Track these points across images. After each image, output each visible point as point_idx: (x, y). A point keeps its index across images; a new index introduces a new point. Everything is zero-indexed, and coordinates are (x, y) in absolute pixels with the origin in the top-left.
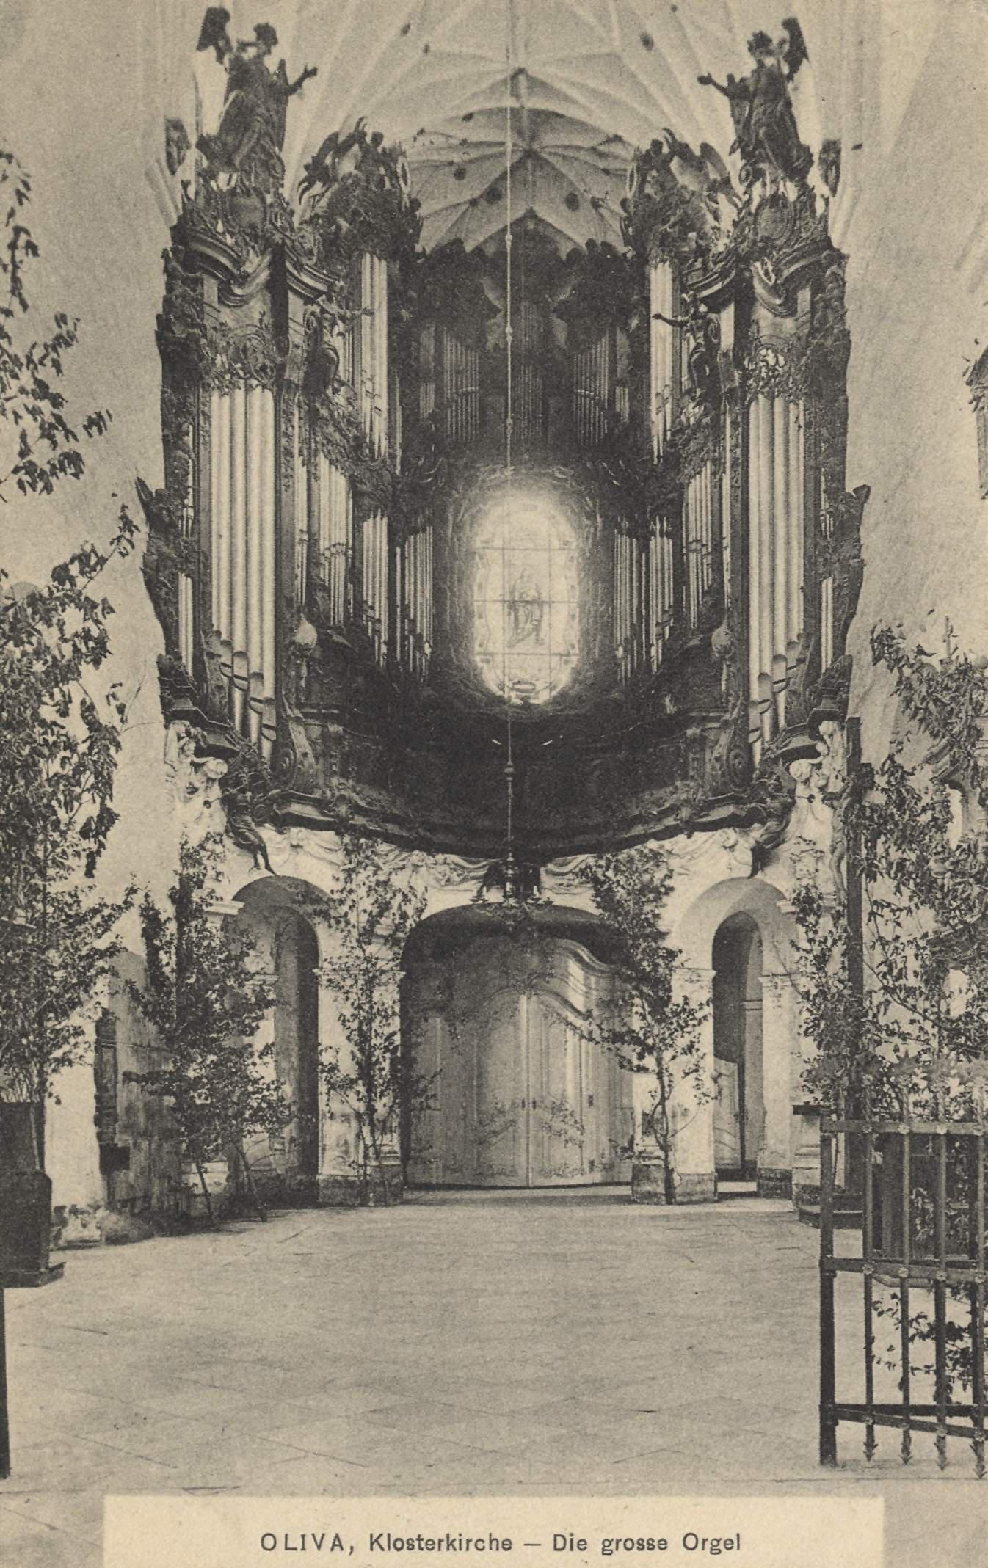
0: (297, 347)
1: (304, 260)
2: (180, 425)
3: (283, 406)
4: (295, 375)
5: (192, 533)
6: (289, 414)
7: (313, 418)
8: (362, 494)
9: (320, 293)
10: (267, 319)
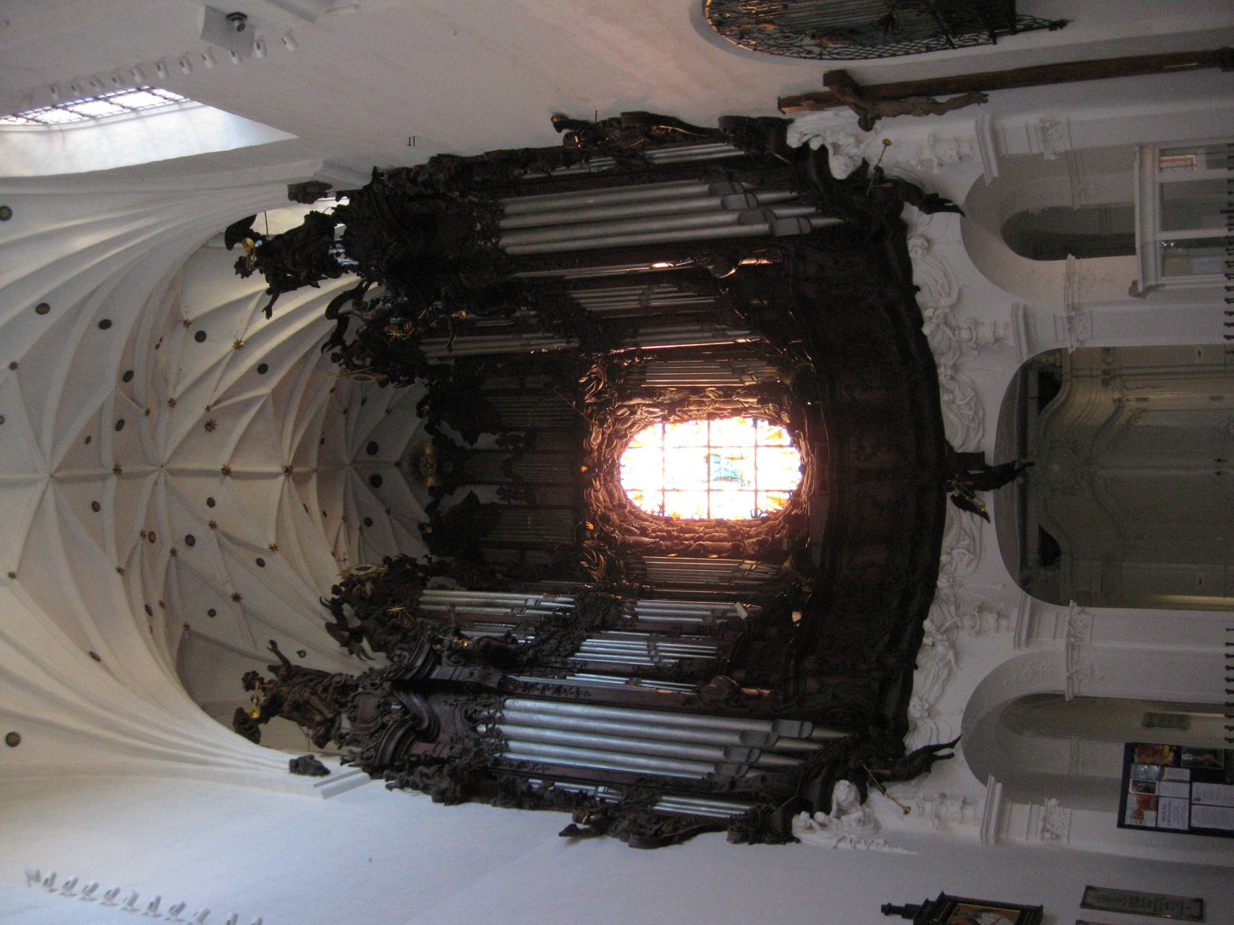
0: (472, 674)
1: (406, 661)
3: (520, 691)
7: (535, 664)
10: (451, 699)
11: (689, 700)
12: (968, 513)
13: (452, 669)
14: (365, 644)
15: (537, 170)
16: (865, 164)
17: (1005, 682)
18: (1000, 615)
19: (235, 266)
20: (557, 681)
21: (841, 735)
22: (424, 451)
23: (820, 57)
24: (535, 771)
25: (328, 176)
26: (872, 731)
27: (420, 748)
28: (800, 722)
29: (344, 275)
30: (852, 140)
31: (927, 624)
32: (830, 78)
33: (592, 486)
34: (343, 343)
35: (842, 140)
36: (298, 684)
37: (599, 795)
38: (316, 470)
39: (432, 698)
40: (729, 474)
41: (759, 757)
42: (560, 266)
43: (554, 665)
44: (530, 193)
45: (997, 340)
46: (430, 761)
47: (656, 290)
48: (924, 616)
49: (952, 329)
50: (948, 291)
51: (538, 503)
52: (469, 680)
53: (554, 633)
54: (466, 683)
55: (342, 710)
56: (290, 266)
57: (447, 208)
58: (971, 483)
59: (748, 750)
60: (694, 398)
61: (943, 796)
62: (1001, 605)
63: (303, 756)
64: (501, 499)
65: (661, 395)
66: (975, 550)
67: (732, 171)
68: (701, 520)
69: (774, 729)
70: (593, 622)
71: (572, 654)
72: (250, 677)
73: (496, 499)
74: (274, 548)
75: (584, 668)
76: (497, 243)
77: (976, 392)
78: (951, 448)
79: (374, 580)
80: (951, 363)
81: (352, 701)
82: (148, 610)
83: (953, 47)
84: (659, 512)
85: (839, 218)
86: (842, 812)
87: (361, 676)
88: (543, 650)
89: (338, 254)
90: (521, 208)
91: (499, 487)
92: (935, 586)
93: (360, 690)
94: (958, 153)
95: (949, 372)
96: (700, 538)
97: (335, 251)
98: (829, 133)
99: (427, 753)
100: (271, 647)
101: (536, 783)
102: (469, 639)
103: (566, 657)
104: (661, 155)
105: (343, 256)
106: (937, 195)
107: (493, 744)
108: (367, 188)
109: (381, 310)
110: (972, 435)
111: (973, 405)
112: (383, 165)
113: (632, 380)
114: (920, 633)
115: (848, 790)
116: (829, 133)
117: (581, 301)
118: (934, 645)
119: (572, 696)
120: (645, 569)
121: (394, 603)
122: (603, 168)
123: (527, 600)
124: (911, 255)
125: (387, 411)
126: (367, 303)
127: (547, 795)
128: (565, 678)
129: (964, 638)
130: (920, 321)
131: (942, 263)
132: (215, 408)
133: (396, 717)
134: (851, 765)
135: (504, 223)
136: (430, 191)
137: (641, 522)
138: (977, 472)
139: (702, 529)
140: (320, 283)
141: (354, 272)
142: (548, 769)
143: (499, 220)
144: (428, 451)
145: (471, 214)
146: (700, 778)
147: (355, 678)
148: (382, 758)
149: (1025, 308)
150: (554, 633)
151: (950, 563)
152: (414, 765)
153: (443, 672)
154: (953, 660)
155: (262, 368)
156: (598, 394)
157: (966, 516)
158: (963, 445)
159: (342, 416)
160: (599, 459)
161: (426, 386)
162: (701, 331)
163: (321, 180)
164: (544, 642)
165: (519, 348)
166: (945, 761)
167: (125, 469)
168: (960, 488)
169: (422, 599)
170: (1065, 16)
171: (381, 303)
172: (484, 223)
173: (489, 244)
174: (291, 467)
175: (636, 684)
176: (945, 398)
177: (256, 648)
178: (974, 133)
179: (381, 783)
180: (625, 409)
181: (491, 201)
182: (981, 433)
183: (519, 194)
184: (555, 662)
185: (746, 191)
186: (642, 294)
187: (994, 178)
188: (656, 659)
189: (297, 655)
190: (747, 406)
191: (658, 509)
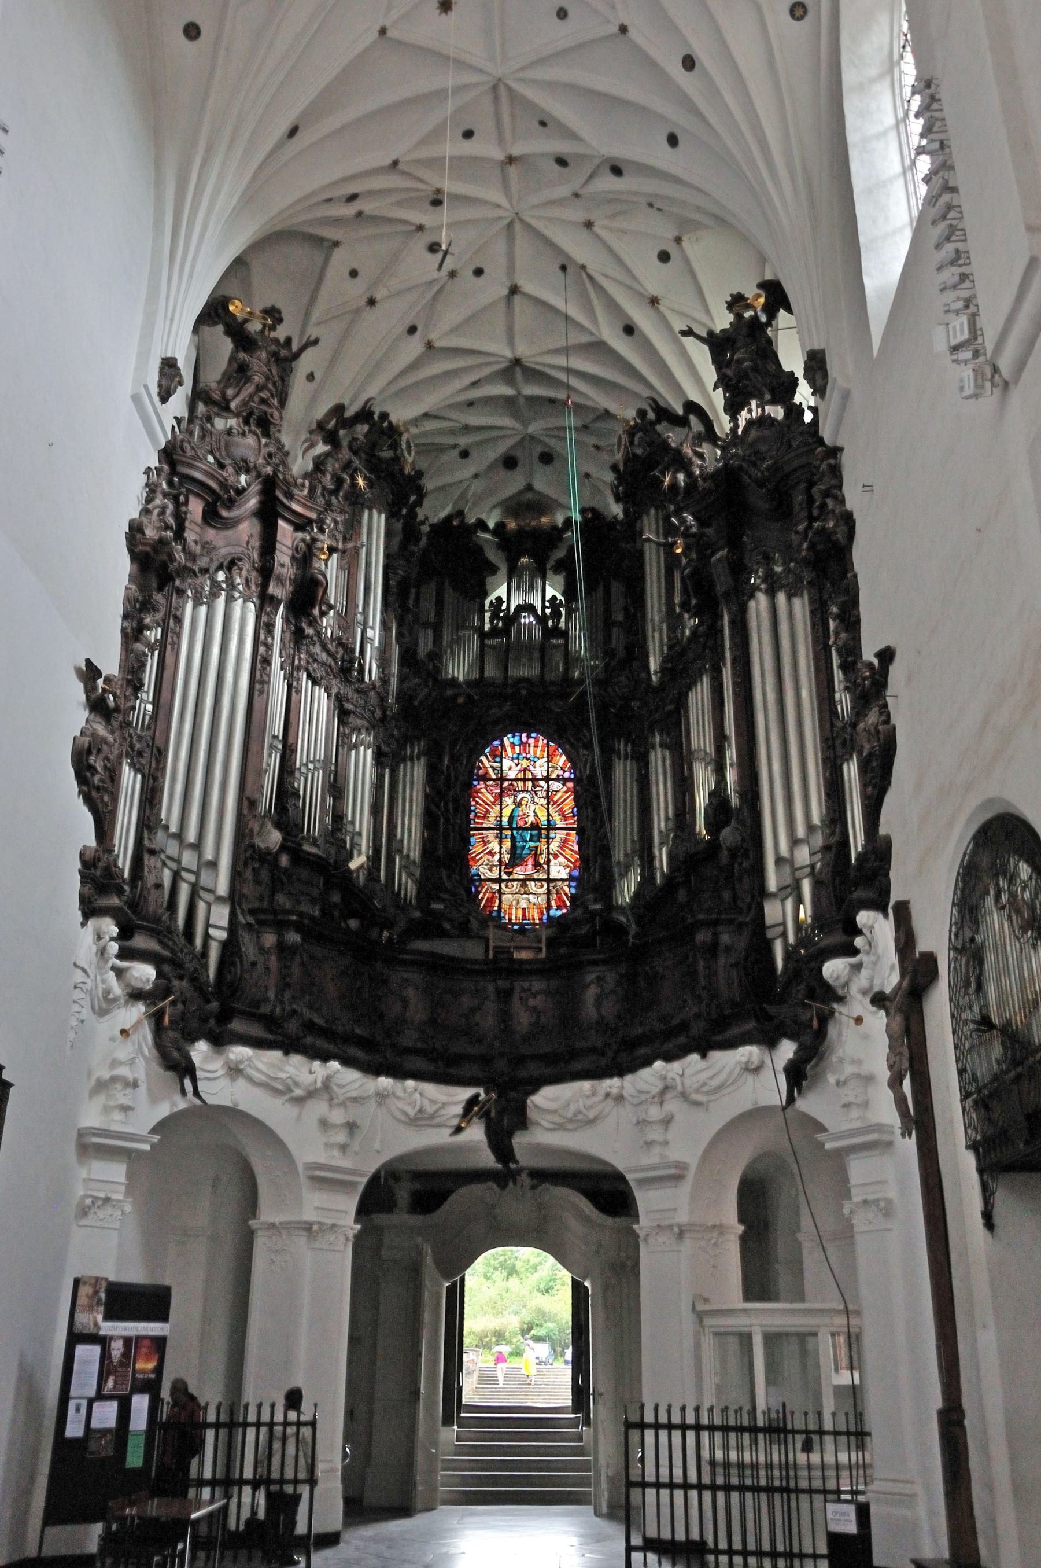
0: (283, 565)
1: (296, 491)
2: (142, 620)
3: (264, 618)
5: (149, 727)
6: (270, 628)
7: (298, 637)
9: (310, 522)
10: (256, 543)
11: (253, 804)
13: (290, 544)
14: (321, 448)
15: (837, 634)
18: (343, 1148)
19: (739, 293)
20: (276, 661)
23: (953, 948)
24: (170, 634)
25: (833, 394)
26: (215, 1005)
27: (196, 508)
29: (728, 418)
31: (334, 1065)
32: (930, 959)
34: (659, 420)
35: (864, 972)
36: (270, 370)
37: (143, 705)
38: (519, 393)
40: (519, 851)
42: (734, 661)
44: (814, 625)
45: (649, 1144)
46: (180, 519)
52: (276, 563)
53: (335, 659)
55: (241, 420)
57: (797, 532)
58: (493, 1114)
59: (195, 869)
63: (183, 372)
67: (834, 849)
68: (469, 821)
69: (219, 899)
70: (348, 700)
71: (309, 676)
72: (277, 315)
74: (429, 346)
75: (292, 689)
76: (760, 590)
79: (397, 459)
81: (250, 431)
82: (353, 197)
83: (964, 1098)
84: (477, 774)
86: (119, 972)
87: (280, 442)
88: (314, 645)
89: (750, 411)
93: (264, 441)
95: (615, 1091)
99: (189, 515)
100: (312, 338)
101: (153, 635)
102: (326, 561)
103: (307, 670)
104: (851, 771)
105: (749, 416)
107: (203, 588)
108: (821, 441)
109: (691, 463)
110: (549, 1117)
111: (580, 1117)
112: (847, 460)
113: (619, 742)
114: (325, 1058)
115: (144, 979)
116: (873, 958)
117: (699, 687)
118: (311, 1072)
121: (365, 478)
122: (839, 708)
123: (372, 628)
127: (139, 647)
128: (282, 669)
129: (318, 1108)
130: (668, 1058)
131: (732, 1084)
132: (585, 276)
133: (232, 479)
134: (176, 983)
135: (781, 598)
136: (815, 513)
139: (459, 822)
141: (731, 430)
142: (173, 649)
145: (792, 560)
146: (163, 816)
147: (277, 435)
148: (184, 463)
151: (405, 1091)
152: (175, 499)
154: (294, 1094)
155: (629, 330)
157: (459, 1110)
158: (536, 1106)
162: (667, 819)
163: (829, 387)
164: (324, 647)
165: (649, 615)
167: (512, 171)
168: (488, 1101)
169: (375, 512)
170: (999, 1230)
175: (271, 747)
176: (586, 1085)
179: (154, 462)
182: (551, 1126)
183: (813, 613)
184: (300, 659)
185: (812, 866)
186: (706, 753)
187: (823, 1145)
188: (303, 770)
189: (309, 371)
191: (481, 772)
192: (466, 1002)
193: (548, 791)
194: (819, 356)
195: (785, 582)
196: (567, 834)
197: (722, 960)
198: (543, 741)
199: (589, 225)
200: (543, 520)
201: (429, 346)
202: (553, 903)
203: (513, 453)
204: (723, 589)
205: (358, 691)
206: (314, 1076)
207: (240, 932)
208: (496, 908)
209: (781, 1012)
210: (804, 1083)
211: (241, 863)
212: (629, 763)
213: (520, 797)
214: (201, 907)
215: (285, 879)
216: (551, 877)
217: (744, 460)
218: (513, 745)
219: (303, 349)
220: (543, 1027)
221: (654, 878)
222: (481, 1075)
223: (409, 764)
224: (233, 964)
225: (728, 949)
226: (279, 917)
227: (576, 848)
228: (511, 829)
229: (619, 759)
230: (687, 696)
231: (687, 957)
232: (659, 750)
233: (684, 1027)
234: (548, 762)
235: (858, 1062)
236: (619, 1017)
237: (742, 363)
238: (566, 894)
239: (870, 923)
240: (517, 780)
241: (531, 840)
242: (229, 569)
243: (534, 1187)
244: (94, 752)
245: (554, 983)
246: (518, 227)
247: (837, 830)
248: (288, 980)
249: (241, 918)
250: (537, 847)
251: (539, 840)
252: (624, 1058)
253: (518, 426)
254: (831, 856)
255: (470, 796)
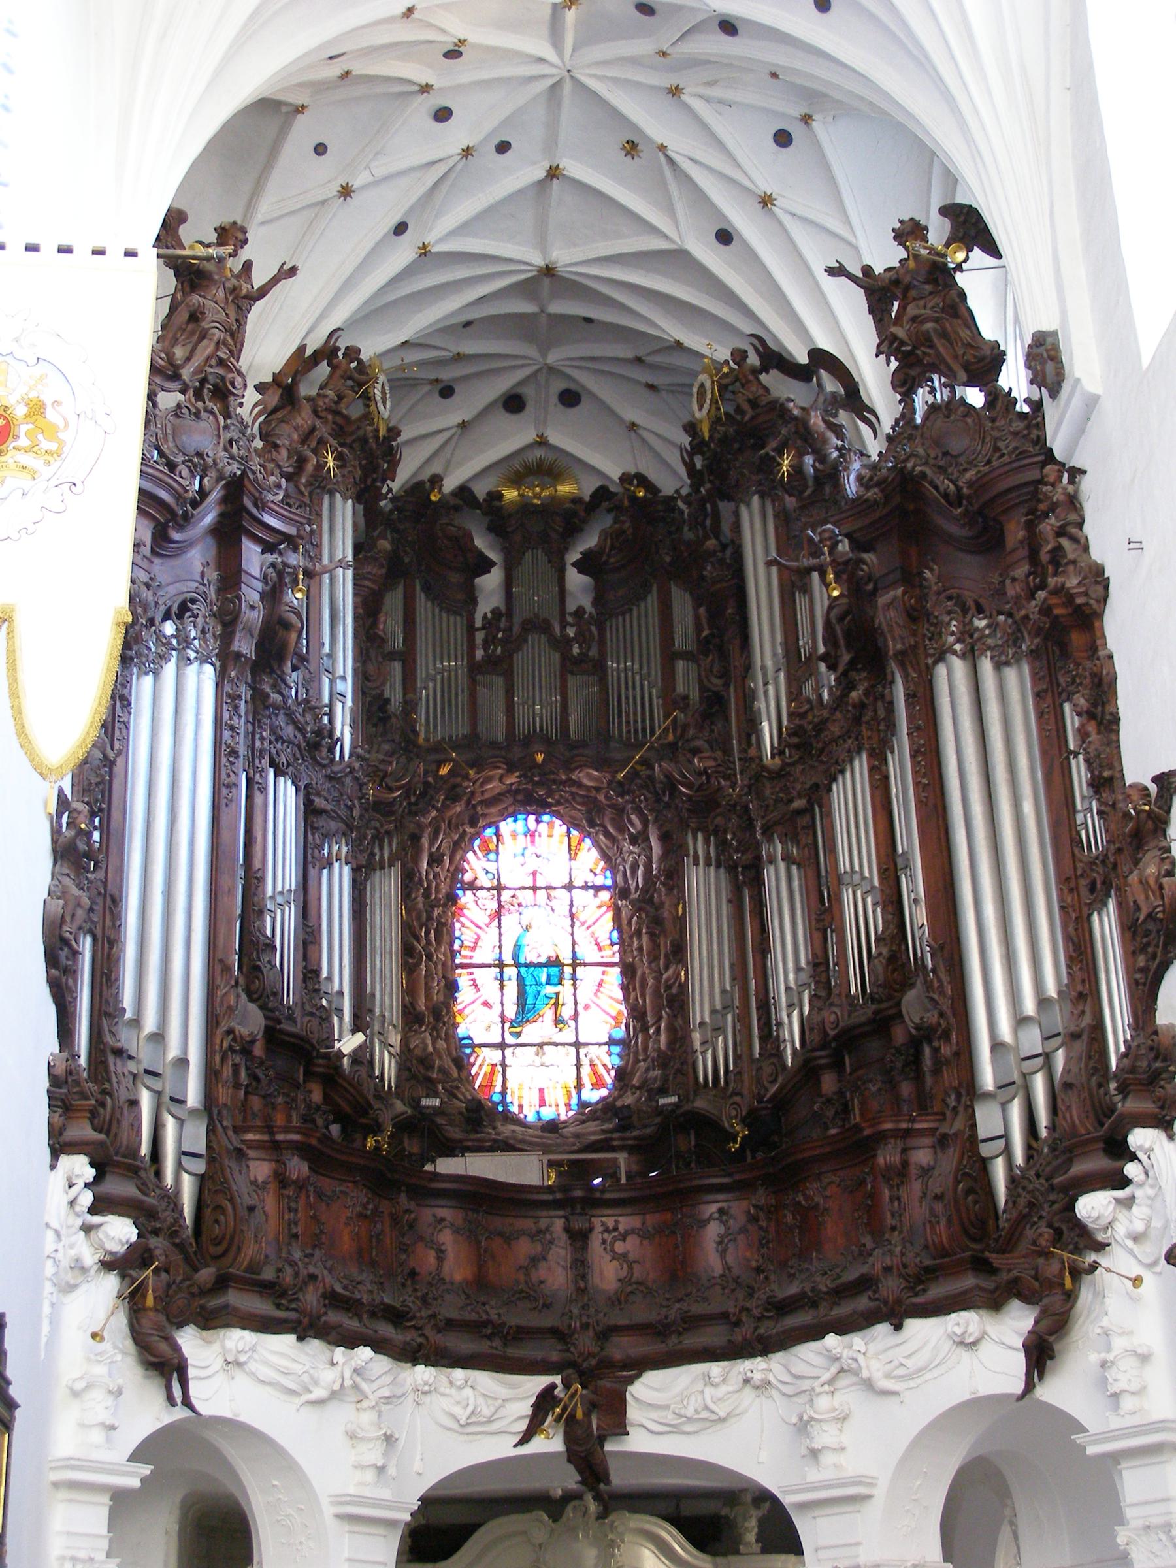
0: (252, 607)
1: (270, 497)
3: (227, 688)
4: (245, 646)
8: (320, 812)
9: (287, 538)
10: (213, 575)
12: (529, 1412)
13: (257, 573)
15: (1082, 734)
16: (1101, 1247)
17: (276, 1483)
18: (381, 1469)
21: (188, 1222)
22: (562, 484)
24: (117, 724)
26: (206, 1274)
28: (203, 1152)
30: (1139, 1227)
31: (365, 1352)
33: (510, 770)
34: (765, 369)
38: (542, 311)
39: (210, 542)
40: (530, 1000)
41: (148, 1088)
43: (258, 736)
44: (1040, 715)
45: (814, 1453)
47: (869, 900)
48: (376, 1350)
49: (831, 1382)
50: (895, 1373)
51: (479, 677)
53: (304, 734)
54: (239, 598)
55: (191, 393)
56: (912, 311)
57: (1014, 580)
58: (579, 1414)
60: (665, 944)
61: (119, 1392)
62: (392, 1471)
64: (485, 617)
65: (670, 889)
66: (469, 1426)
67: (1085, 1037)
68: (453, 954)
69: (193, 1112)
70: (318, 794)
71: (272, 763)
72: (240, 236)
73: (484, 608)
74: (424, 251)
76: (955, 653)
77: (722, 1420)
78: (631, 1380)
79: (367, 417)
80: (771, 1378)
81: (206, 410)
84: (462, 882)
85: (1006, 1203)
88: (277, 715)
89: (933, 391)
90: (1014, 695)
91: (503, 609)
92: (415, 1361)
94: (1122, 1391)
95: (757, 1377)
96: (429, 957)
97: (937, 384)
98: (1151, 1192)
100: (285, 267)
105: (930, 400)
106: (1052, 1358)
109: (825, 441)
110: (654, 1415)
111: (705, 1414)
112: (1088, 487)
113: (695, 839)
114: (350, 1342)
116: (1151, 1192)
117: (848, 775)
119: (224, 776)
120: (382, 868)
121: (339, 457)
122: (1083, 833)
124: (953, 1315)
125: (633, 426)
126: (836, 416)
129: (343, 1415)
130: (843, 1328)
137: (448, 853)
138: (595, 1427)
139: (441, 957)
140: (883, 357)
143: (992, 658)
144: (564, 489)
145: (1000, 613)
147: (239, 410)
149: (867, 1498)
150: (304, 734)
153: (253, 558)
155: (725, 237)
156: (671, 785)
157: (525, 1408)
159: (630, 354)
160: (554, 782)
161: (677, 491)
162: (798, 969)
163: (1066, 387)
164: (291, 718)
165: (759, 663)
166: (164, 1391)
168: (573, 1396)
171: (840, 443)
172: (987, 632)
173: (951, 639)
174: (553, 275)
176: (716, 1369)
177: (262, 223)
178: (1156, 1416)
180: (639, 826)
181: (1024, 647)
183: (1038, 695)
184: (262, 739)
186: (863, 878)
188: (270, 905)
190: (651, 1031)
191: (468, 877)
192: (524, 1248)
193: (571, 906)
194: (1049, 340)
195: (990, 641)
196: (604, 973)
197: (916, 1186)
198: (560, 828)
199: (675, 91)
200: (559, 488)
201: (424, 251)
202: (587, 1080)
203: (520, 390)
204: (899, 646)
205: (330, 778)
206: (338, 1368)
207: (226, 1162)
208: (498, 1089)
209: (1014, 1264)
210: (1049, 1362)
211: (217, 1058)
212: (712, 869)
213: (528, 915)
214: (170, 1124)
215: (261, 1075)
216: (581, 1040)
217: (926, 463)
218: (514, 835)
219: (274, 281)
220: (638, 1283)
221: (779, 1055)
222: (555, 1356)
223: (378, 872)
224: (219, 1208)
225: (926, 1171)
226: (280, 1137)
227: (619, 995)
228: (517, 965)
229: (696, 863)
230: (830, 790)
231: (862, 1183)
232: (782, 866)
233: (865, 1284)
234: (571, 859)
235: (1131, 1333)
236: (758, 1270)
237: (922, 323)
238: (604, 1065)
239: (1147, 1145)
240: (524, 888)
241: (548, 983)
242: (180, 617)
243: (602, 1516)
244: (68, 919)
245: (652, 1220)
246: (568, 87)
247: (1088, 1009)
248: (294, 1231)
249: (225, 1142)
250: (558, 994)
251: (560, 983)
252: (769, 1328)
253: (531, 351)
254: (1080, 1046)
255: (453, 914)
